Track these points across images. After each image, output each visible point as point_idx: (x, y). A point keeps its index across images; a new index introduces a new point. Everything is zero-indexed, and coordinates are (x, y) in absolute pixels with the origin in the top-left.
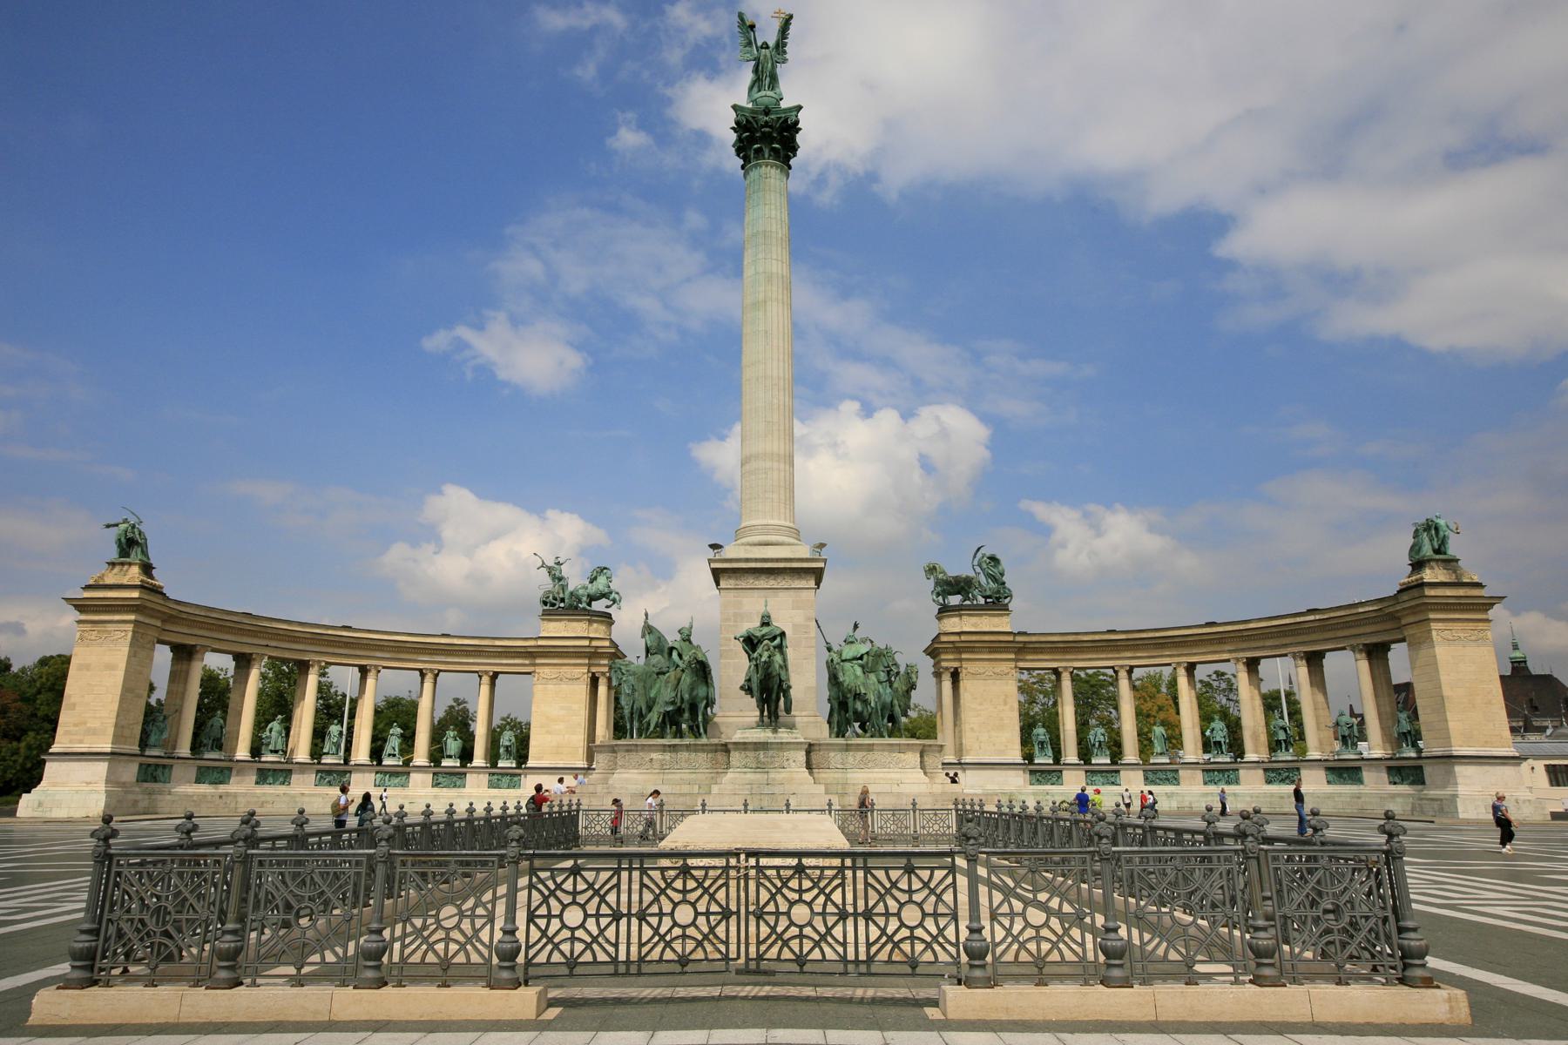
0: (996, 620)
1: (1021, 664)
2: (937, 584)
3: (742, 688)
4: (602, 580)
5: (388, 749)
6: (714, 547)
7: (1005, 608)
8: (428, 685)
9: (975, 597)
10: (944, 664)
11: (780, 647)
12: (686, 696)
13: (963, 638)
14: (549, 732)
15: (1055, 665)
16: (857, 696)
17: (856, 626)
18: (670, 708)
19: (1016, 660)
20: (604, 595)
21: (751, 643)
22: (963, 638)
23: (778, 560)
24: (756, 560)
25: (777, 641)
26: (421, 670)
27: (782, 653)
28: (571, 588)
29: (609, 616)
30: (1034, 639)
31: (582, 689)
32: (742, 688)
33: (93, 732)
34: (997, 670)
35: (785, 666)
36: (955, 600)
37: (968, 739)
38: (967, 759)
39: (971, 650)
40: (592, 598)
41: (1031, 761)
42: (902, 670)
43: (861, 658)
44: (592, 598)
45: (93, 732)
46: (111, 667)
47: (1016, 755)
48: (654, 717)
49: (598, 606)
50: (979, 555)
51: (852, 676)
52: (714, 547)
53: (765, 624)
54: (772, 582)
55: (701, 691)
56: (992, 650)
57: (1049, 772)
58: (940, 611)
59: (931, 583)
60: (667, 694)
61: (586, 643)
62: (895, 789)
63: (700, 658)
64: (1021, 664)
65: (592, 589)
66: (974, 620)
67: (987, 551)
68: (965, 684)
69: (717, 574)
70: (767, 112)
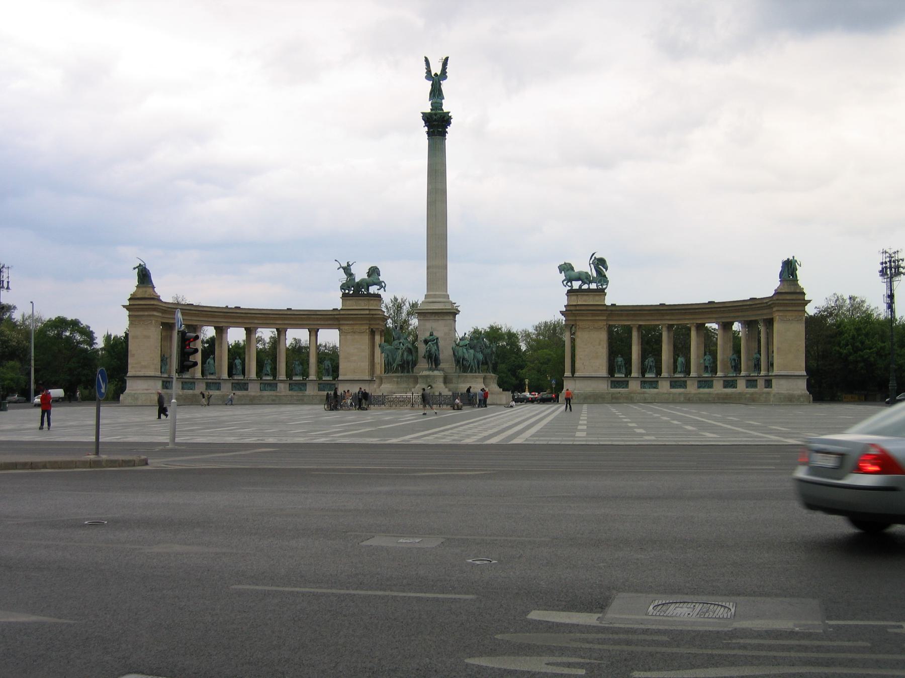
0: (597, 298)
5: (264, 371)
7: (601, 292)
16: (464, 359)
28: (357, 280)
29: (379, 296)
31: (366, 338)
33: (145, 367)
39: (582, 315)
41: (612, 376)
45: (145, 367)
46: (147, 337)
47: (604, 372)
48: (395, 365)
51: (461, 352)
53: (431, 335)
54: (436, 318)
56: (593, 315)
58: (569, 291)
59: (562, 276)
60: (399, 358)
61: (367, 312)
64: (611, 323)
66: (585, 298)
67: (597, 256)
68: (579, 334)
70: (436, 114)
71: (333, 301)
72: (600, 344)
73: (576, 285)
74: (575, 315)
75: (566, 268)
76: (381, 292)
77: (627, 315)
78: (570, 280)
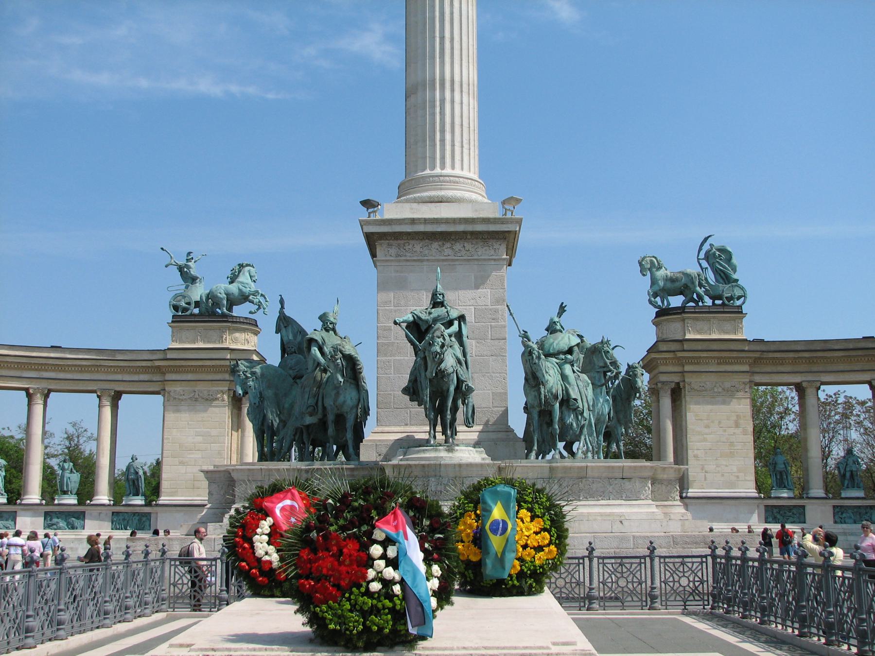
0: (728, 326)
1: (758, 378)
2: (654, 282)
3: (406, 391)
4: (244, 278)
6: (368, 204)
7: (739, 311)
8: (38, 409)
9: (700, 298)
10: (663, 378)
11: (459, 335)
12: (329, 402)
13: (686, 346)
14: (182, 463)
15: (797, 379)
16: (567, 402)
17: (562, 309)
18: (309, 420)
19: (754, 373)
20: (244, 298)
21: (418, 330)
22: (686, 346)
23: (454, 221)
24: (426, 221)
25: (455, 327)
26: (27, 390)
27: (462, 344)
30: (773, 348)
32: (406, 391)
34: (727, 385)
35: (463, 361)
36: (676, 301)
37: (693, 468)
38: (692, 492)
39: (697, 361)
40: (232, 302)
42: (623, 369)
43: (570, 351)
44: (232, 302)
49: (239, 311)
50: (706, 247)
52: (368, 204)
55: (349, 397)
56: (722, 361)
57: (790, 508)
58: (658, 315)
62: (617, 527)
63: (349, 349)
64: (758, 378)
65: (234, 288)
66: (700, 325)
67: (716, 242)
69: (372, 240)
71: (155, 334)
72: (737, 426)
73: (676, 301)
74: (681, 362)
75: (648, 267)
76: (258, 316)
77: (795, 361)
78: (660, 291)
